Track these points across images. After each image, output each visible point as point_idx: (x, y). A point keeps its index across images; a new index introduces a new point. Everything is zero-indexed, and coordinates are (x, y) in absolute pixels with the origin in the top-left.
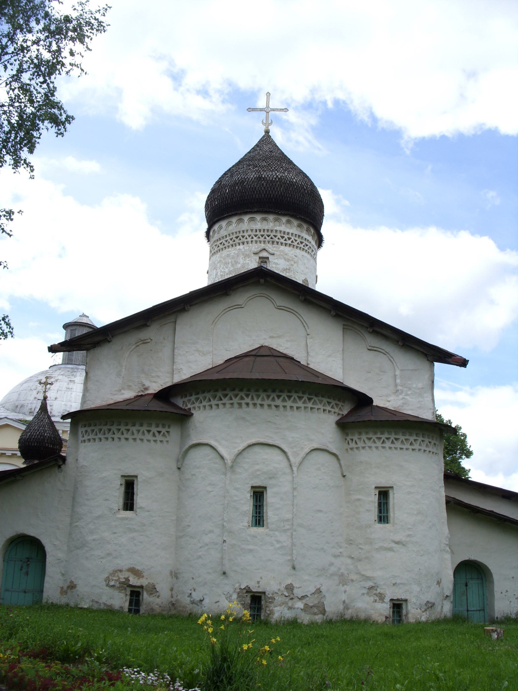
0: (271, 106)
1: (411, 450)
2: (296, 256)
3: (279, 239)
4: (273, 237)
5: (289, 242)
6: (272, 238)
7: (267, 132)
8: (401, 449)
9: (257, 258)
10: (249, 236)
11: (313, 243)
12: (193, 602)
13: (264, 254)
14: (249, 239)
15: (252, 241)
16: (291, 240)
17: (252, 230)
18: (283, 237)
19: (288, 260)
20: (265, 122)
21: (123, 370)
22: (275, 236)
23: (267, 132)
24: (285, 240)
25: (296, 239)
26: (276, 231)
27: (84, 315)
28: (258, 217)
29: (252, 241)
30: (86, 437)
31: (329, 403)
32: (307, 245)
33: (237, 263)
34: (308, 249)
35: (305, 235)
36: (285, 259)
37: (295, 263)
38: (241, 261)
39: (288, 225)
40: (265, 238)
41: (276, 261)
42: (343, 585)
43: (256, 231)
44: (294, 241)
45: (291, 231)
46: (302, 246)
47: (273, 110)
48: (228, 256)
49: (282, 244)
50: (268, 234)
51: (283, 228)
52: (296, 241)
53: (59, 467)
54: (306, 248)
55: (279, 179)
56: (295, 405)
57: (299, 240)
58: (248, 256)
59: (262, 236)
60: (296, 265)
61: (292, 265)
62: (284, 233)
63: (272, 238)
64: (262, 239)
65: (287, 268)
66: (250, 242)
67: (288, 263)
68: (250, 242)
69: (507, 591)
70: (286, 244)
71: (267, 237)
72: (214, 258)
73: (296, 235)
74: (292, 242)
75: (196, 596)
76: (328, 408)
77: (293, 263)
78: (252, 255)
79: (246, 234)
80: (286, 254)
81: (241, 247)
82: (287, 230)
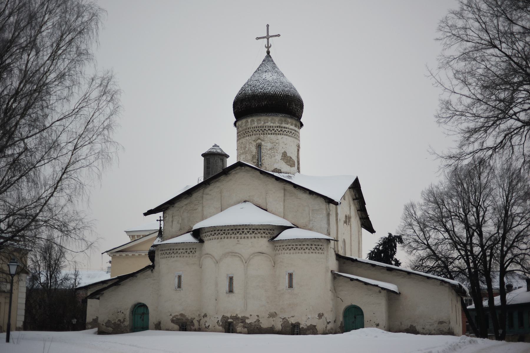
0: (270, 34)
1: (303, 253)
2: (277, 139)
3: (267, 131)
4: (264, 130)
5: (273, 132)
6: (263, 131)
7: (268, 52)
8: (299, 253)
9: (255, 144)
10: (251, 131)
11: (293, 127)
12: (206, 327)
13: (259, 141)
14: (251, 133)
15: (253, 134)
16: (274, 130)
17: (253, 128)
18: (269, 130)
19: (273, 143)
20: (267, 46)
21: (180, 220)
22: (265, 130)
23: (268, 52)
24: (271, 131)
25: (278, 129)
26: (266, 127)
27: (215, 146)
28: (255, 119)
29: (253, 134)
30: (162, 256)
31: (264, 233)
32: (285, 131)
33: (246, 147)
34: (287, 132)
35: (284, 125)
36: (270, 142)
37: (277, 143)
38: (248, 146)
39: (273, 121)
40: (260, 131)
41: (266, 144)
42: (273, 318)
43: (255, 128)
44: (276, 130)
45: (274, 125)
46: (282, 132)
47: (271, 36)
48: (242, 143)
49: (269, 134)
50: (261, 129)
51: (269, 124)
52: (277, 130)
53: (152, 270)
54: (285, 133)
55: (265, 94)
56: (246, 236)
57: (279, 129)
58: (251, 143)
59: (258, 130)
60: (277, 144)
61: (275, 145)
62: (270, 127)
63: (263, 131)
64: (258, 132)
65: (272, 148)
66: (252, 135)
67: (272, 145)
68: (252, 135)
69: (370, 321)
70: (271, 134)
71: (260, 131)
72: (241, 141)
73: (277, 127)
74: (275, 131)
75: (207, 325)
76: (264, 235)
77: (275, 144)
78: (253, 142)
79: (250, 130)
80: (271, 140)
81: (248, 138)
82: (272, 125)
